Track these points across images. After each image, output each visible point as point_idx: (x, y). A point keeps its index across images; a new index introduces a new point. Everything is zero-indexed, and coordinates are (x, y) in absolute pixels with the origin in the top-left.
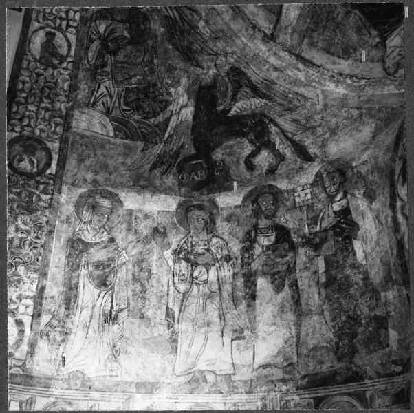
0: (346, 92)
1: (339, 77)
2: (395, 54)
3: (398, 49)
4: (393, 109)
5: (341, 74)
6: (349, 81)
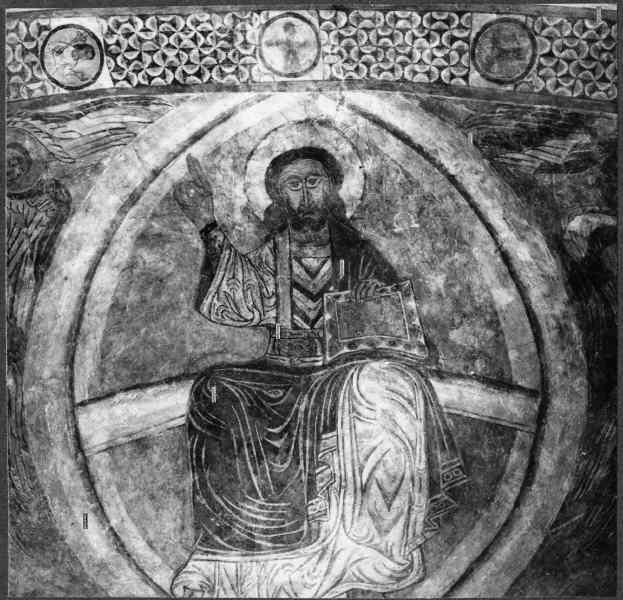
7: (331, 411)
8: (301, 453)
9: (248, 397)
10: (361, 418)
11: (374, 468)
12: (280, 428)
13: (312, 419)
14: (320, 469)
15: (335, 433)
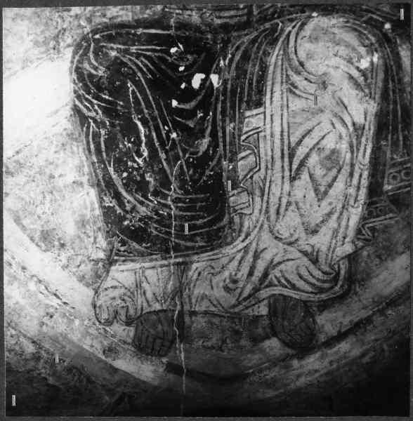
0: (22, 302)
1: (20, 271)
2: (116, 293)
3: (123, 290)
4: (89, 380)
5: (24, 268)
6: (32, 286)
7: (258, 82)
8: (220, 134)
9: (146, 66)
10: (297, 92)
11: (307, 156)
12: (193, 104)
13: (234, 92)
14: (243, 154)
15: (261, 110)
